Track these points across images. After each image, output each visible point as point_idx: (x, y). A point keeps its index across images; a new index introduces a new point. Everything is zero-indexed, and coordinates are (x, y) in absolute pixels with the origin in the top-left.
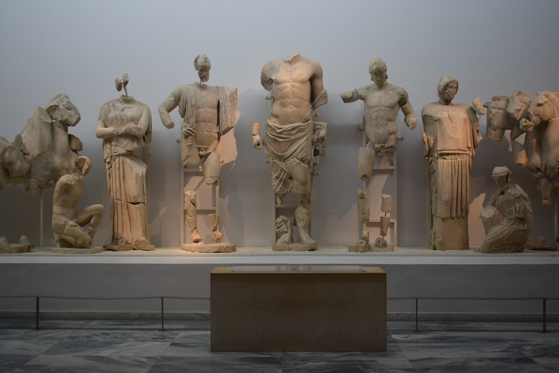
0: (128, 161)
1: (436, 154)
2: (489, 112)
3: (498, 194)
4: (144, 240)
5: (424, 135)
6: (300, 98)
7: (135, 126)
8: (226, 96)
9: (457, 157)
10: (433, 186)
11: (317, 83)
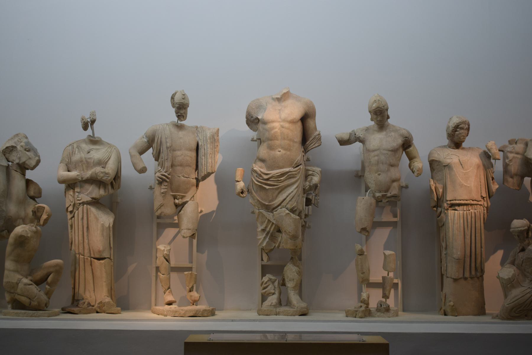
0: (93, 210)
1: (445, 205)
2: (505, 157)
3: (518, 251)
4: (109, 302)
5: (432, 182)
6: (290, 140)
7: (103, 170)
8: (206, 137)
9: (470, 208)
10: (443, 241)
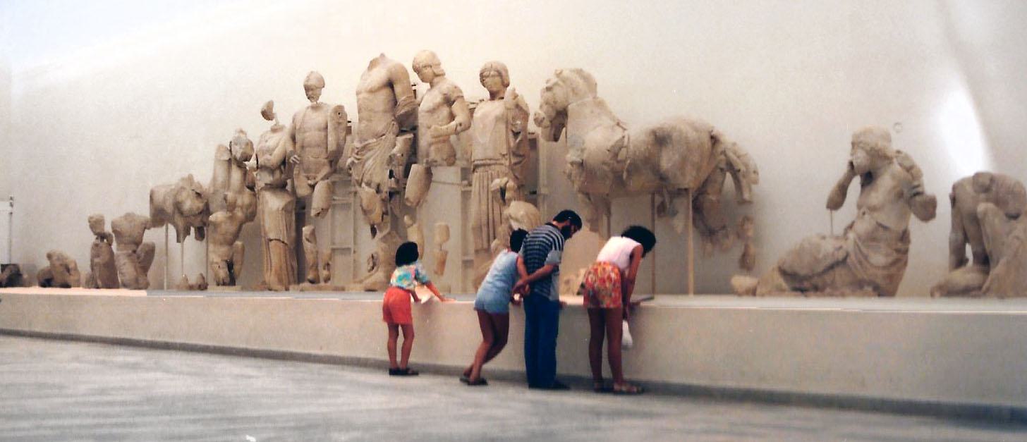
11: (398, 89)
